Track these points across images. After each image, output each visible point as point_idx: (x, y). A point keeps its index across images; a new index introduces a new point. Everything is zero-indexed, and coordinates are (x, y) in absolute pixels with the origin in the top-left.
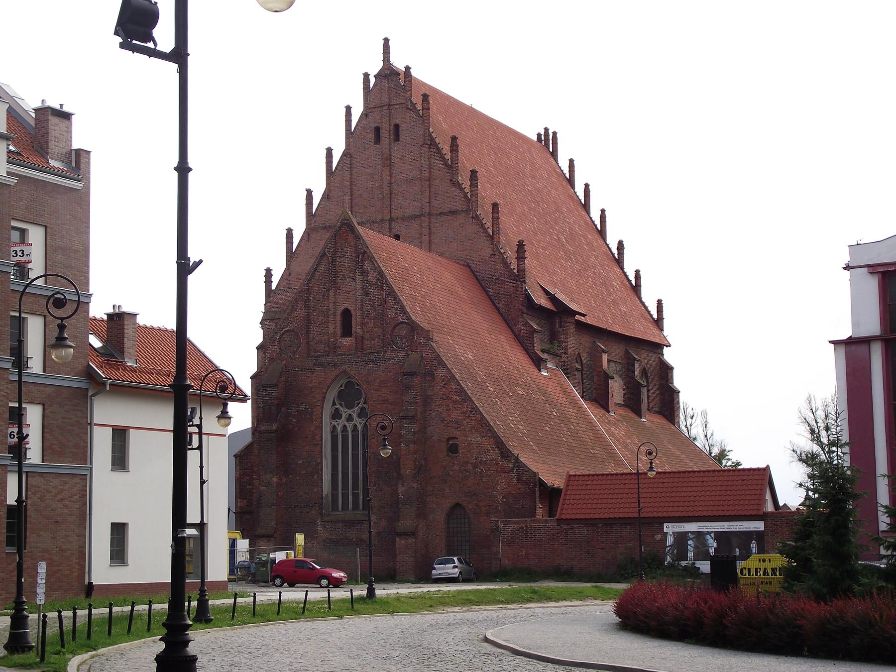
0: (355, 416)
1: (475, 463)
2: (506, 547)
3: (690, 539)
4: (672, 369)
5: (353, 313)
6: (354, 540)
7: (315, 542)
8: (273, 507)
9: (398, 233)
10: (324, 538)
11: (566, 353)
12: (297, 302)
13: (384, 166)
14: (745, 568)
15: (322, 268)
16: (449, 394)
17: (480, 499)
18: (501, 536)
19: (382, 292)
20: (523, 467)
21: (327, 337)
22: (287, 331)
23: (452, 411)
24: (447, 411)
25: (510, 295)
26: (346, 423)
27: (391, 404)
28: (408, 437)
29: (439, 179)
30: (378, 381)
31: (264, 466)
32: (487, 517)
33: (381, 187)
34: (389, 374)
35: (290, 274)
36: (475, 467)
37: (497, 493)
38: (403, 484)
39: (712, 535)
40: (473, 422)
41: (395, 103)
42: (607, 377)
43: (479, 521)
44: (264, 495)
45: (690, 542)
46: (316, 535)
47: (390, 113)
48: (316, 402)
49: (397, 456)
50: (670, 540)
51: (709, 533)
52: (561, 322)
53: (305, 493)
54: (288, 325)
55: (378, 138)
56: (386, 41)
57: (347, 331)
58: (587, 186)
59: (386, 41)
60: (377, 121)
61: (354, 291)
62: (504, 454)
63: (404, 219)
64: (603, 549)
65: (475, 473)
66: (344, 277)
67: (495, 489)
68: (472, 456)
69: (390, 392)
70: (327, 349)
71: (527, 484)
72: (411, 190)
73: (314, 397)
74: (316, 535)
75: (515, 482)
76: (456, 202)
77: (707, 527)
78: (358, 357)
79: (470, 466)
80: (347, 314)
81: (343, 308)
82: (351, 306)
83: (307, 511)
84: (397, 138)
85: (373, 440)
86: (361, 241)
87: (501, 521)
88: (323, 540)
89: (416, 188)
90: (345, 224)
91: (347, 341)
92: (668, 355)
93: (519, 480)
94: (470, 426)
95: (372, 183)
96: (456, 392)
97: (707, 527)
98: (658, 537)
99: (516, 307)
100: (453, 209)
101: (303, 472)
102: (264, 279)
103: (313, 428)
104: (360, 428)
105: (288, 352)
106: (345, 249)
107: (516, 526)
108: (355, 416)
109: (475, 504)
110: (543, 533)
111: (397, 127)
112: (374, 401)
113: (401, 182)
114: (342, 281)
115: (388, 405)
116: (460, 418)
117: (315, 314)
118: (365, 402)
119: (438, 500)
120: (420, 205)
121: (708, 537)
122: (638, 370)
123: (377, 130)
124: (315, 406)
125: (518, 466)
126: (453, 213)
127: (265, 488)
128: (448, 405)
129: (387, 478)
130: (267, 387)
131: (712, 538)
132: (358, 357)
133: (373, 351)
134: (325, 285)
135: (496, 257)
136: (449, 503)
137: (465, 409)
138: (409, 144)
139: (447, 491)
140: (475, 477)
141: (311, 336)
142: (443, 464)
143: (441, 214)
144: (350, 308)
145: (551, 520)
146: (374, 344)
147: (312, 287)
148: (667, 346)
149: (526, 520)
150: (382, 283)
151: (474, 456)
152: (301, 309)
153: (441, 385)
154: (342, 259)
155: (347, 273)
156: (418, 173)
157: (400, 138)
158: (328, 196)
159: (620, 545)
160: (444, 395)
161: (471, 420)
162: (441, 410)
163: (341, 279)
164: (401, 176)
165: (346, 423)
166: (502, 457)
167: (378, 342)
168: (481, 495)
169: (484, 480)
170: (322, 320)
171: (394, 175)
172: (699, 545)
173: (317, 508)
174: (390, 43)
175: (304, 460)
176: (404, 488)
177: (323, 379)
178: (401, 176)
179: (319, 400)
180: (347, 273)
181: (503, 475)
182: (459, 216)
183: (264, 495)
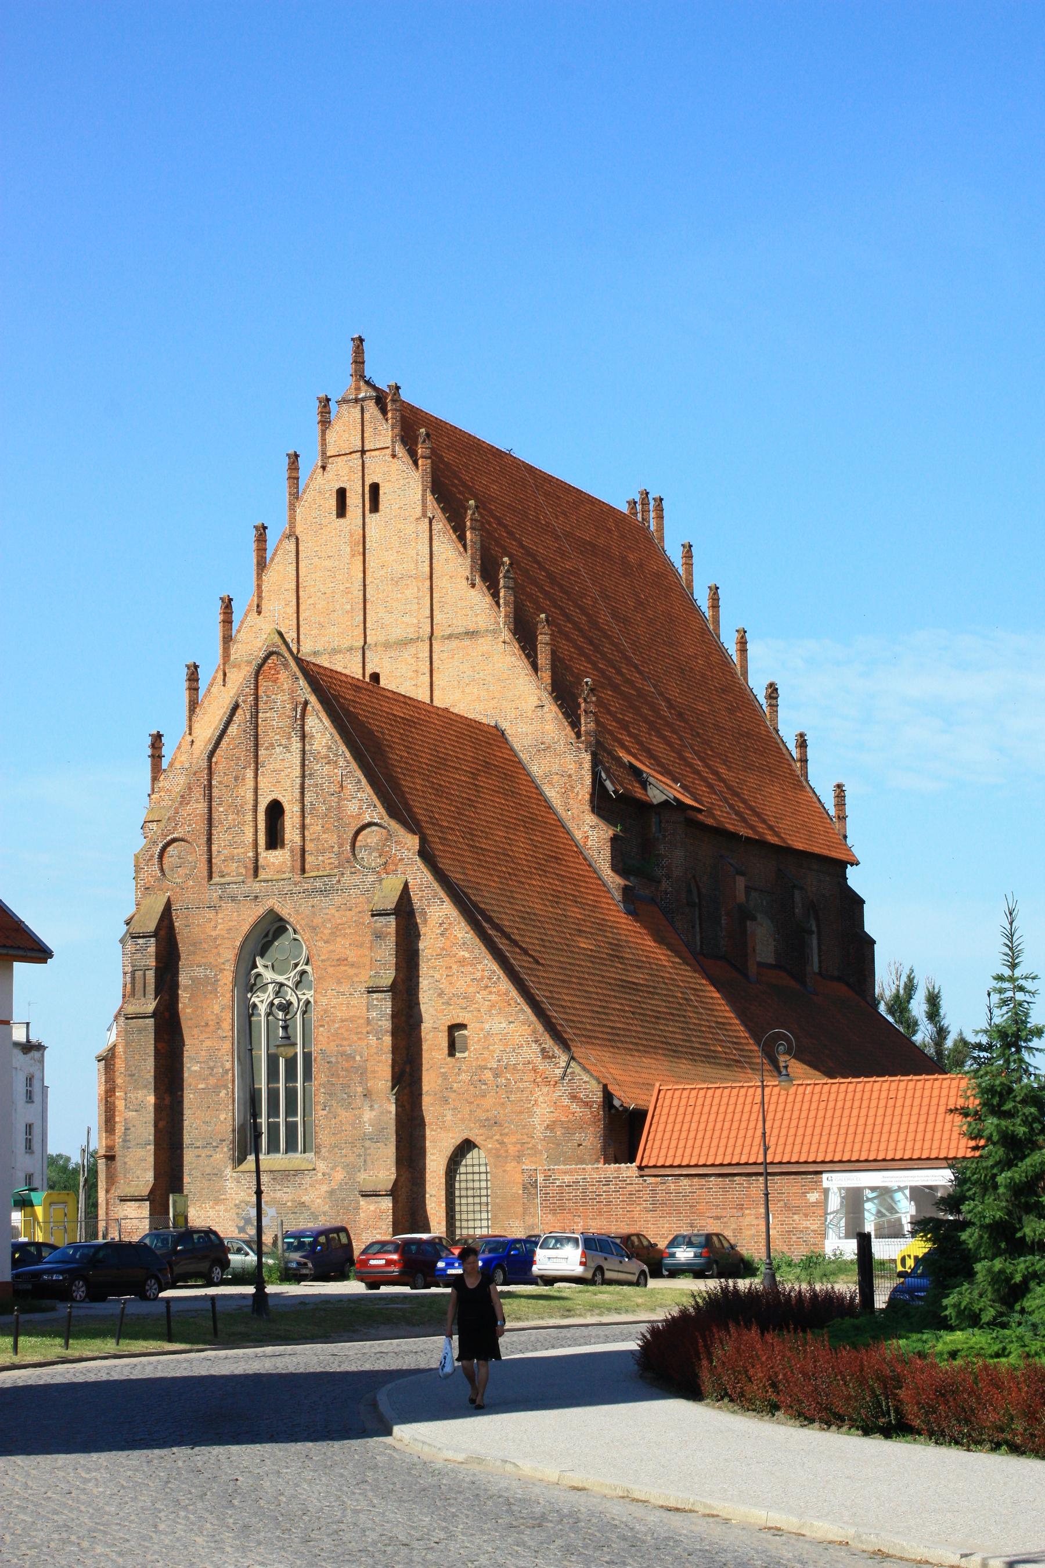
1: (497, 1068)
2: (550, 1216)
3: (868, 1200)
4: (863, 902)
5: (286, 807)
6: (289, 1204)
7: (222, 1207)
8: (148, 1147)
9: (377, 670)
10: (237, 1202)
11: (668, 876)
12: (190, 788)
13: (353, 555)
14: (909, 1256)
15: (233, 729)
16: (452, 947)
17: (507, 1130)
18: (541, 1197)
19: (336, 771)
20: (580, 1075)
21: (242, 850)
22: (174, 840)
23: (457, 978)
24: (449, 978)
25: (570, 776)
27: (352, 965)
28: (380, 1023)
29: (448, 577)
30: (329, 925)
31: (134, 1075)
32: (518, 1163)
33: (347, 591)
34: (348, 913)
35: (193, 742)
36: (496, 1076)
37: (536, 1120)
38: (371, 1106)
39: (907, 1192)
41: (372, 448)
42: (744, 915)
43: (504, 1171)
44: (134, 1126)
45: (868, 1206)
46: (223, 1197)
48: (223, 964)
49: (361, 1057)
50: (834, 1202)
51: (900, 1189)
52: (660, 822)
53: (204, 1122)
54: (175, 829)
55: (342, 510)
58: (714, 590)
60: (342, 479)
61: (289, 770)
62: (548, 1052)
63: (387, 645)
64: (718, 1218)
65: (497, 1087)
66: (272, 745)
67: (531, 1114)
68: (493, 1057)
69: (350, 944)
70: (243, 871)
71: (587, 1104)
72: (399, 595)
73: (219, 954)
74: (223, 1197)
75: (566, 1101)
76: (477, 615)
77: (898, 1179)
78: (296, 884)
79: (488, 1075)
80: (275, 810)
81: (269, 799)
82: (284, 796)
83: (209, 1153)
84: (375, 508)
85: (321, 1029)
87: (540, 1170)
88: (236, 1205)
89: (407, 592)
90: (271, 653)
92: (855, 878)
93: (574, 1097)
94: (487, 1003)
95: (333, 585)
96: (464, 944)
97: (898, 1179)
98: (813, 1197)
99: (580, 797)
101: (201, 1086)
102: (149, 752)
103: (217, 1009)
105: (176, 876)
106: (273, 697)
107: (567, 1178)
109: (497, 1140)
110: (613, 1191)
111: (375, 488)
112: (323, 961)
113: (382, 581)
114: (268, 752)
115: (346, 968)
116: (471, 990)
117: (221, 809)
119: (433, 1133)
120: (415, 621)
121: (898, 1196)
122: (800, 905)
123: (342, 494)
124: (222, 970)
125: (571, 1073)
126: (472, 634)
127: (134, 1113)
128: (451, 967)
129: (345, 1096)
130: (139, 937)
131: (907, 1198)
132: (296, 884)
133: (321, 873)
134: (238, 759)
135: (546, 709)
136: (452, 1138)
137: (478, 975)
138: (395, 516)
139: (449, 1118)
140: (497, 1093)
141: (214, 848)
142: (442, 1070)
143: (450, 637)
145: (627, 1167)
146: (323, 862)
147: (216, 763)
148: (852, 865)
149: (584, 1169)
150: (336, 755)
151: (495, 1055)
152: (197, 801)
153: (438, 931)
154: (268, 715)
155: (277, 737)
156: (413, 566)
157: (381, 507)
158: (258, 606)
159: (747, 1212)
160: (443, 949)
161: (491, 993)
162: (437, 976)
163: (267, 749)
164: (382, 573)
166: (544, 1057)
167: (330, 858)
168: (507, 1124)
169: (513, 1097)
170: (234, 820)
171: (371, 570)
172: (884, 1211)
173: (225, 1149)
175: (203, 1065)
176: (374, 1113)
177: (236, 923)
178: (382, 573)
179: (228, 961)
180: (277, 737)
181: (545, 1089)
182: (481, 640)
183: (134, 1126)
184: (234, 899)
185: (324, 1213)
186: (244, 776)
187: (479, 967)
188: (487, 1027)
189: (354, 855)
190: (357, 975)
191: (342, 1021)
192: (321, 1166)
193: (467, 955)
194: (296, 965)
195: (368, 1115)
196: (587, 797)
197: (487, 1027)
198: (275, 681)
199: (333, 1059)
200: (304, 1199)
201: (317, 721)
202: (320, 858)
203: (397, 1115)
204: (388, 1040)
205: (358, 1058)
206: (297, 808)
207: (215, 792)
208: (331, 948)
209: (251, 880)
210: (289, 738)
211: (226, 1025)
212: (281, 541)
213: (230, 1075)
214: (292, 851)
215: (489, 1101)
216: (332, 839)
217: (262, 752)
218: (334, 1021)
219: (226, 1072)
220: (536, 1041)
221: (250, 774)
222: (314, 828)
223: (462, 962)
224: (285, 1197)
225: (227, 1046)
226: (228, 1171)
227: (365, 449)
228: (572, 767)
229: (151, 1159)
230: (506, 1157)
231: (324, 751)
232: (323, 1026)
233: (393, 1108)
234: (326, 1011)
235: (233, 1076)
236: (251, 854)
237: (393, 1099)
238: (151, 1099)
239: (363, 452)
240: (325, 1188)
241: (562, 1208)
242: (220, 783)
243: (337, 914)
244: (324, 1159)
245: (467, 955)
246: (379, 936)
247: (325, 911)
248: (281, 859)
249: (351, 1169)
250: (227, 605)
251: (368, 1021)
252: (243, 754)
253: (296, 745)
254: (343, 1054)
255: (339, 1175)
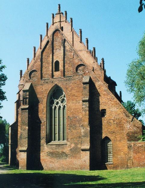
0: (60, 102)
2: (135, 154)
5: (60, 62)
7: (43, 153)
12: (37, 59)
15: (48, 46)
26: (56, 106)
27: (76, 96)
30: (70, 87)
36: (114, 121)
40: (113, 103)
47: (60, 24)
56: (59, 5)
57: (57, 69)
59: (59, 5)
70: (49, 77)
73: (43, 95)
79: (112, 121)
80: (57, 63)
81: (56, 60)
85: (68, 111)
86: (64, 35)
91: (57, 74)
96: (105, 90)
100: (81, 50)
104: (62, 107)
107: (140, 145)
108: (60, 102)
111: (62, 27)
118: (64, 97)
127: (23, 131)
137: (109, 97)
141: (43, 72)
144: (58, 60)
161: (112, 102)
163: (55, 50)
165: (56, 106)
174: (60, 5)
184: (47, 83)
185: (69, 154)
186: (49, 57)
187: (109, 96)
188: (111, 109)
189: (77, 72)
190: (77, 99)
191: (74, 109)
192: (68, 143)
193: (106, 93)
194: (61, 98)
195: (82, 131)
196: (103, 78)
197: (111, 109)
198: (57, 36)
199: (71, 118)
200: (64, 151)
201: (67, 43)
202: (68, 73)
203: (90, 130)
204: (88, 112)
205: (78, 118)
206: (62, 62)
207: (43, 60)
208: (71, 92)
209: (51, 78)
210: (60, 47)
211: (45, 111)
212: (45, 37)
213: (46, 122)
214: (61, 71)
215: (112, 127)
216: (71, 69)
217: (54, 51)
218: (72, 110)
219: (45, 122)
220: (124, 113)
221: (51, 55)
222: (66, 66)
223: (104, 95)
224: (59, 151)
225: (45, 116)
226: (45, 145)
227: (61, 21)
228: (100, 73)
229: (27, 142)
230: (117, 140)
231: (69, 50)
232: (69, 111)
233: (89, 129)
234: (69, 107)
235: (46, 123)
236: (51, 73)
237: (89, 127)
238: (27, 128)
239: (60, 22)
240: (69, 149)
241: (139, 152)
242: (44, 58)
243: (72, 85)
244: (69, 141)
245: (106, 93)
246: (85, 88)
247: (69, 84)
248: (58, 74)
249: (76, 144)
250: (41, 36)
251: (83, 108)
252: (50, 52)
253: (62, 48)
254: (74, 117)
255: (73, 145)
